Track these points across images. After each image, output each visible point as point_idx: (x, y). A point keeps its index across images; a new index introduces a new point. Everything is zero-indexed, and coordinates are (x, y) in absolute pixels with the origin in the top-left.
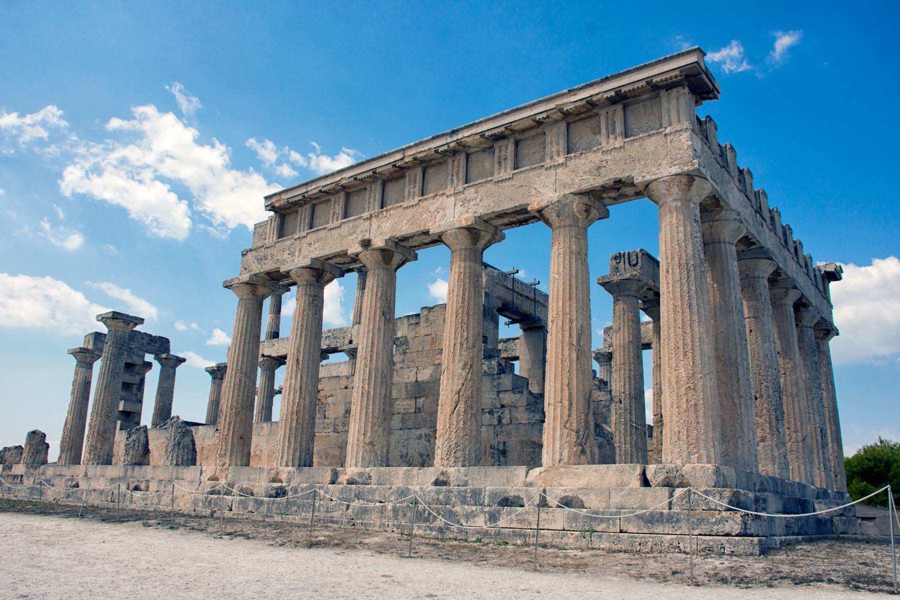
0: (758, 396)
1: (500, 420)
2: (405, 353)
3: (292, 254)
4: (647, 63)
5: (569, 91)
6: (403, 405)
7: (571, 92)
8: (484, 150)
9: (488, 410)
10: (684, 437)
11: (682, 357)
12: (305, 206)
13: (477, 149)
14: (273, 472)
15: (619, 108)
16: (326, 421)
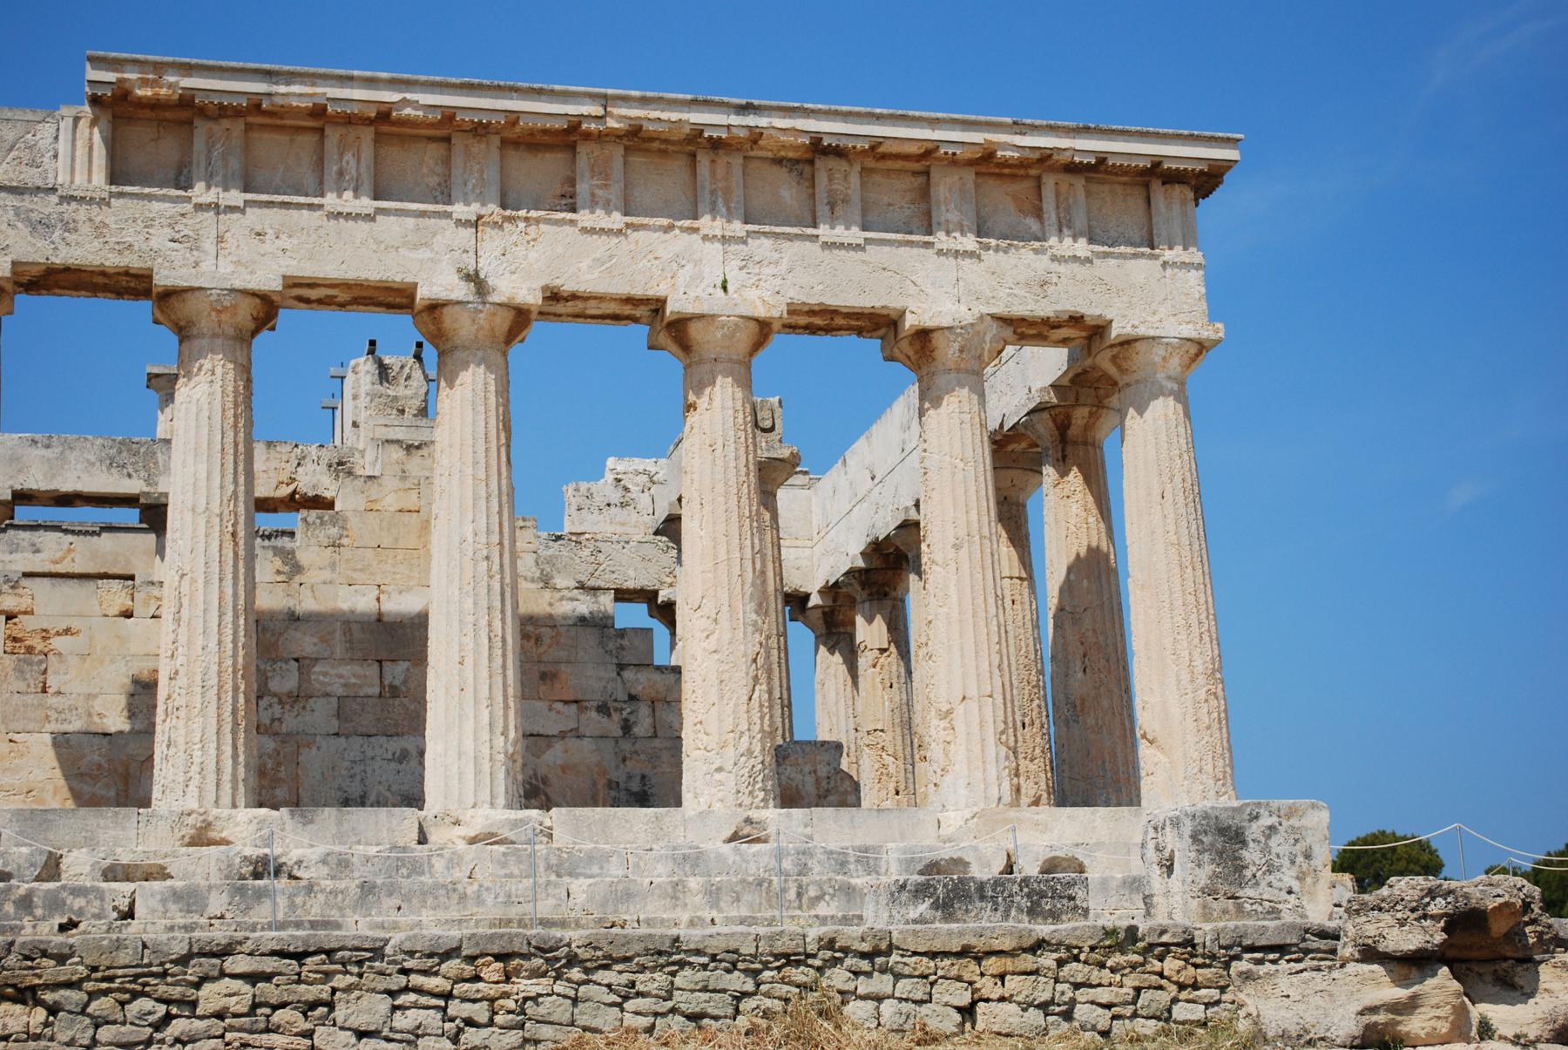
0: (1027, 721)
1: (627, 727)
2: (335, 545)
3: (194, 243)
4: (1161, 131)
5: (1015, 123)
6: (341, 676)
7: (1018, 127)
8: (778, 161)
9: (595, 704)
10: (1209, 768)
11: (1197, 640)
12: (225, 123)
13: (770, 155)
14: (190, 820)
15: (1079, 182)
16: (51, 700)
